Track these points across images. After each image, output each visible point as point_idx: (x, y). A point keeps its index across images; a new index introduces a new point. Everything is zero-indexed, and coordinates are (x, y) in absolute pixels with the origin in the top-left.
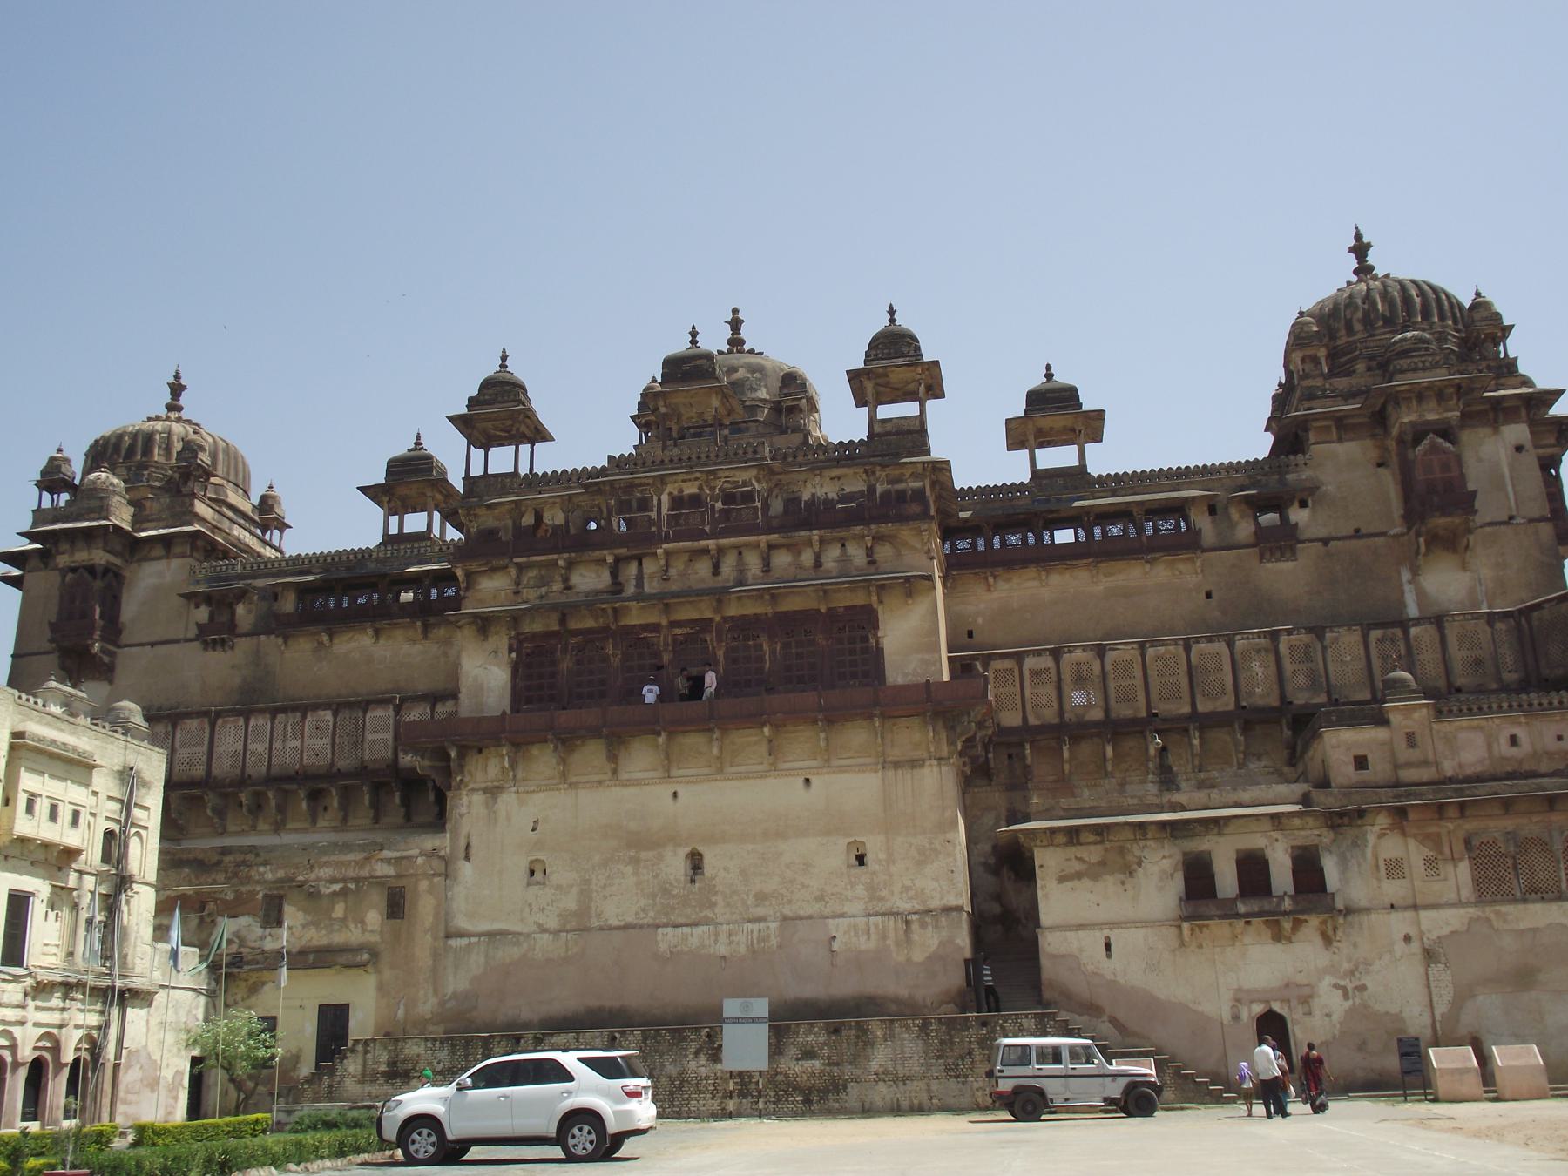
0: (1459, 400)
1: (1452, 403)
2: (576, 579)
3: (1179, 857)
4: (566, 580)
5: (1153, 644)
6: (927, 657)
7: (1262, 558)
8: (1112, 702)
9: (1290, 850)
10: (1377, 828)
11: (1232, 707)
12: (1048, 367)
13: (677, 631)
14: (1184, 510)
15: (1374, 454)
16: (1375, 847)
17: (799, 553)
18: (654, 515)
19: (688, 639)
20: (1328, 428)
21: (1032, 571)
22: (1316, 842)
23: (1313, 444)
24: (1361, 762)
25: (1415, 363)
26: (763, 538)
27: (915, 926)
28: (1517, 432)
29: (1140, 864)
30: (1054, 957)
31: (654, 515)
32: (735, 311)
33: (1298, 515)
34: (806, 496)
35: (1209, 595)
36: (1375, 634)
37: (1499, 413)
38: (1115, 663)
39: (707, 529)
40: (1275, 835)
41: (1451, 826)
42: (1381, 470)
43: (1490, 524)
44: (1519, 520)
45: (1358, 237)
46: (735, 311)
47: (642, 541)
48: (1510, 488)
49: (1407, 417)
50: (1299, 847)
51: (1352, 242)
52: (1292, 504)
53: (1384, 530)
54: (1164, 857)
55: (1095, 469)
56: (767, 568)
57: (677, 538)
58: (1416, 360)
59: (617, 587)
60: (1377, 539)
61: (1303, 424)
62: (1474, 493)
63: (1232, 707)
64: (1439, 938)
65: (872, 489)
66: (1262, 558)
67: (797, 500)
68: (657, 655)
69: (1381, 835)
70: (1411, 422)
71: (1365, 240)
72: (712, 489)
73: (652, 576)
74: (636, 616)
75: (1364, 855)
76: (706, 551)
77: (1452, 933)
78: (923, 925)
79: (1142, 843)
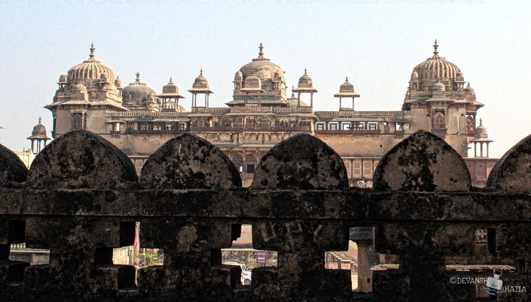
1: (445, 104)
2: (221, 137)
4: (219, 137)
5: (365, 159)
7: (395, 137)
8: (353, 174)
12: (347, 78)
13: (247, 153)
15: (427, 113)
17: (278, 136)
18: (242, 124)
19: (249, 155)
20: (416, 104)
21: (337, 136)
26: (270, 133)
28: (462, 110)
31: (242, 124)
32: (261, 44)
34: (281, 121)
35: (381, 146)
39: (256, 129)
42: (428, 117)
43: (452, 134)
44: (459, 134)
45: (436, 43)
46: (261, 44)
47: (238, 130)
48: (458, 125)
49: (434, 107)
51: (434, 44)
56: (270, 138)
57: (248, 130)
59: (232, 141)
61: (410, 104)
65: (297, 121)
66: (395, 137)
67: (278, 122)
68: (242, 158)
70: (435, 109)
71: (437, 44)
72: (257, 118)
73: (241, 138)
74: (236, 149)
76: (255, 134)
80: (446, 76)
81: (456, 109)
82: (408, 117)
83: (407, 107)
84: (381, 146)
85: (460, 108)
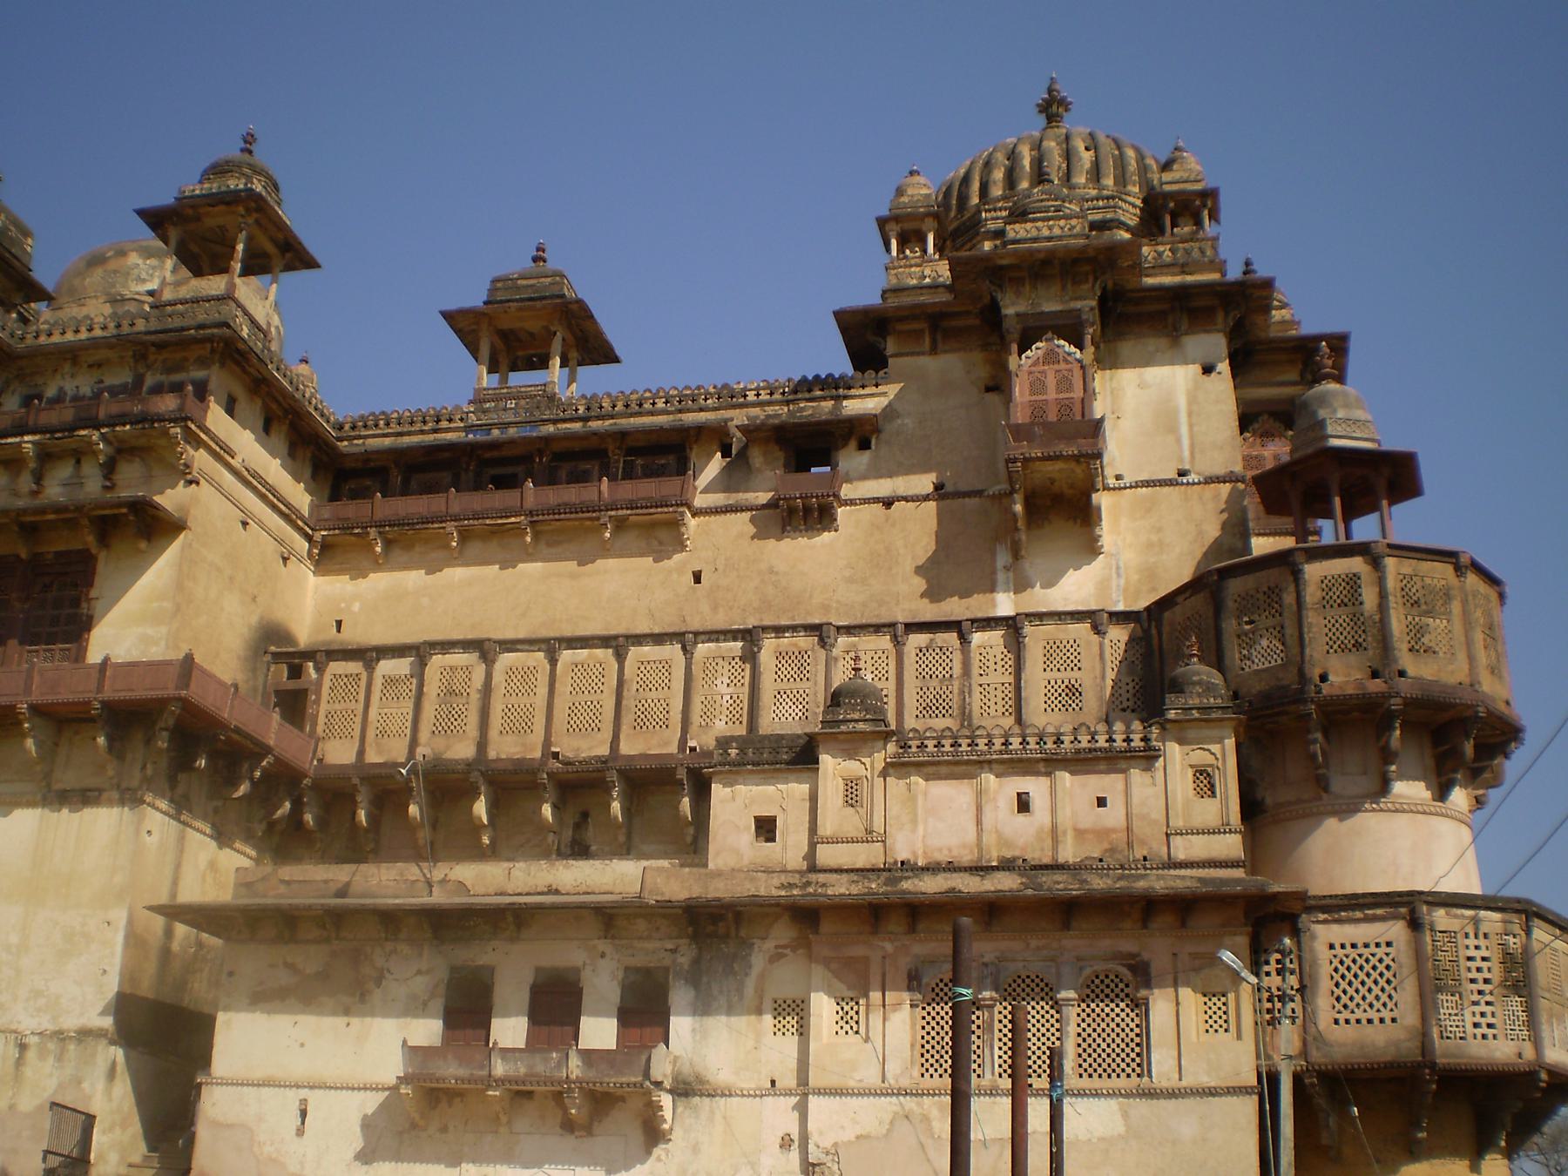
0: (1096, 279)
3: (442, 974)
6: (150, 631)
8: (493, 733)
9: (620, 975)
10: (769, 945)
11: (673, 749)
12: (540, 249)
14: (685, 451)
16: (762, 977)
22: (667, 962)
23: (892, 356)
25: (1038, 229)
27: (31, 1055)
29: (379, 981)
30: (217, 1124)
35: (697, 578)
36: (917, 640)
38: (510, 671)
40: (603, 945)
41: (889, 947)
43: (1147, 484)
44: (1193, 477)
48: (1184, 430)
50: (637, 970)
52: (845, 445)
53: (979, 487)
54: (419, 972)
58: (1040, 224)
60: (967, 500)
62: (1101, 421)
63: (673, 749)
64: (835, 1145)
69: (776, 958)
70: (1018, 315)
75: (740, 990)
77: (858, 1137)
78: (42, 1055)
79: (389, 946)
81: (1163, 342)
84: (697, 578)
85: (1191, 331)
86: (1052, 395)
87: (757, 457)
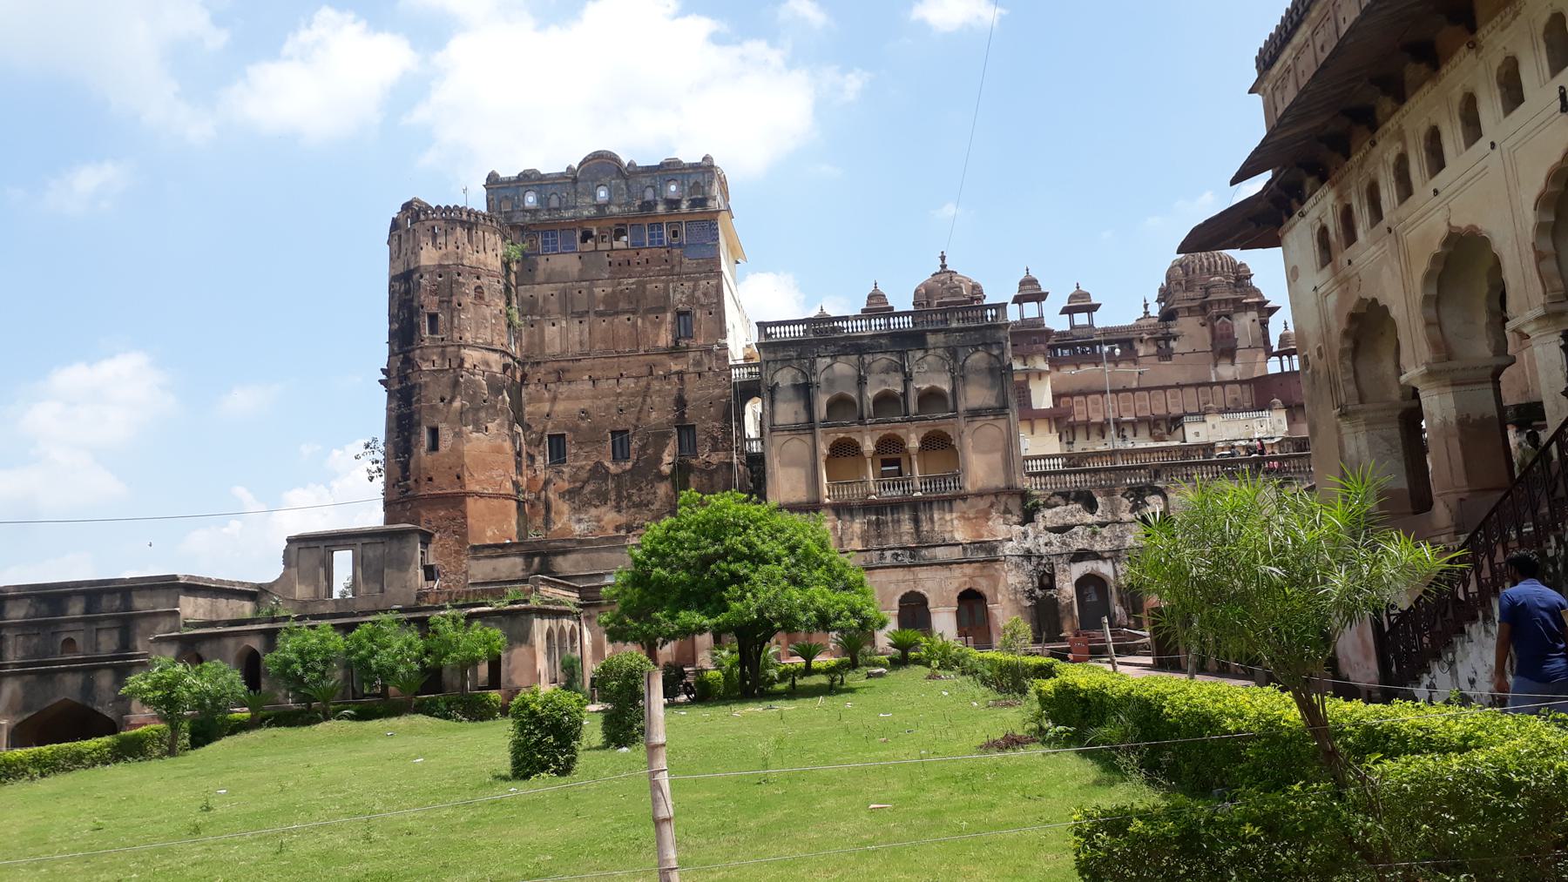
24: (1197, 434)
28: (1253, 315)
33: (1173, 344)
37: (1248, 307)
49: (1215, 311)
55: (1098, 325)
80: (1222, 268)
82: (1175, 329)
83: (1168, 316)
86: (1224, 332)
87: (1150, 343)
